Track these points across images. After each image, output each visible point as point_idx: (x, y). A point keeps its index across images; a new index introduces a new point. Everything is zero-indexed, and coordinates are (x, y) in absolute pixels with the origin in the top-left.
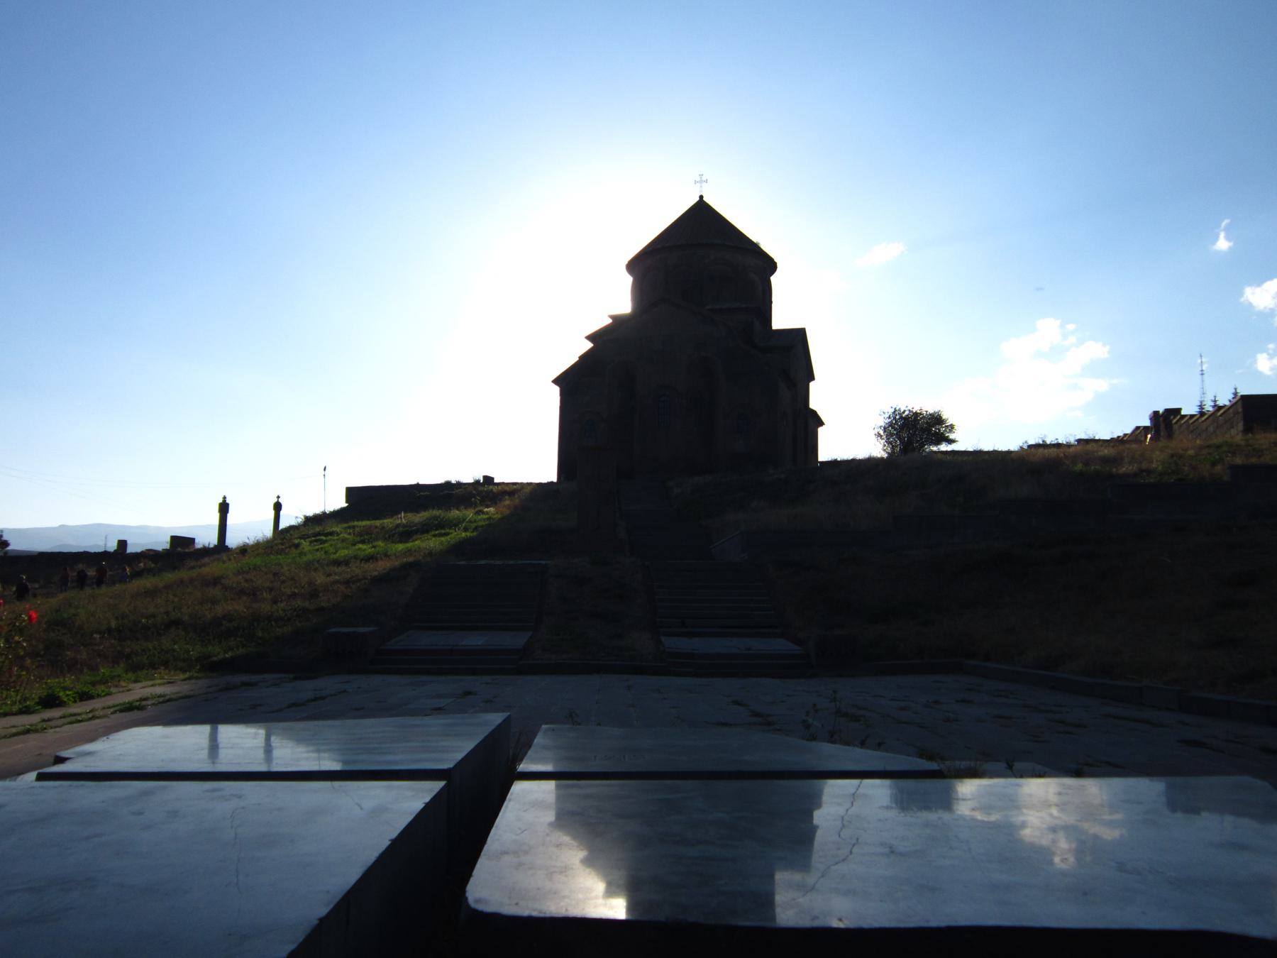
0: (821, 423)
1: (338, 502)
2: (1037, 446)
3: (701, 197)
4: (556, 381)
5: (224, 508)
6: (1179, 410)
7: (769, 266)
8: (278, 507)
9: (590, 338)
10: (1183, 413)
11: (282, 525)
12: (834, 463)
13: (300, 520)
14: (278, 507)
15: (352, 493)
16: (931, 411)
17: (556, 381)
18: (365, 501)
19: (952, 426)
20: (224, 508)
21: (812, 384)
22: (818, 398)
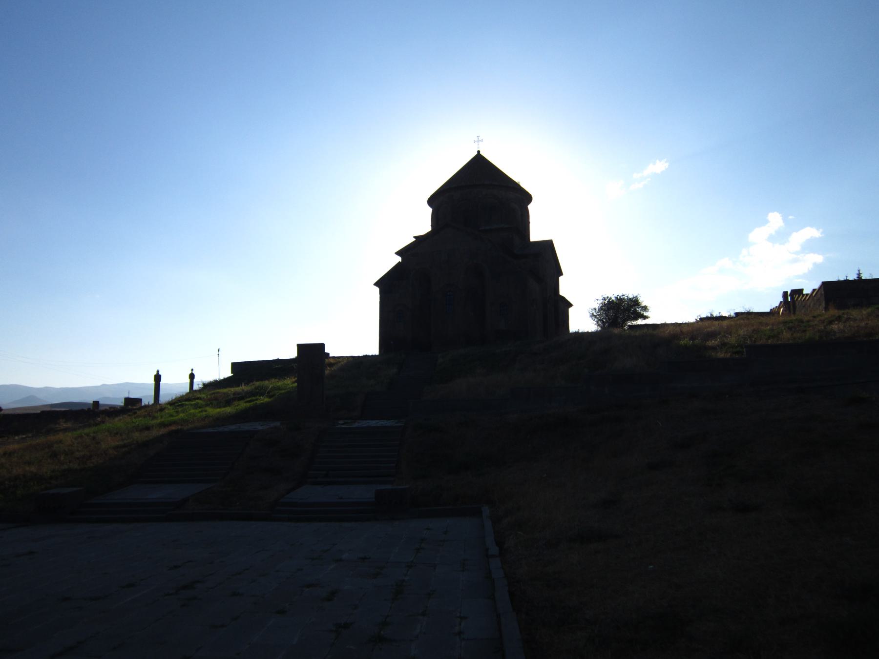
0: (571, 305)
1: (227, 373)
2: (707, 318)
3: (479, 152)
4: (376, 284)
5: (158, 378)
6: (802, 290)
7: (527, 198)
8: (192, 376)
9: (398, 253)
10: (805, 292)
11: (196, 387)
12: (577, 334)
13: (201, 386)
14: (192, 376)
15: (235, 366)
16: (631, 296)
17: (376, 284)
18: (244, 371)
19: (645, 308)
20: (158, 378)
21: (561, 278)
22: (566, 288)
